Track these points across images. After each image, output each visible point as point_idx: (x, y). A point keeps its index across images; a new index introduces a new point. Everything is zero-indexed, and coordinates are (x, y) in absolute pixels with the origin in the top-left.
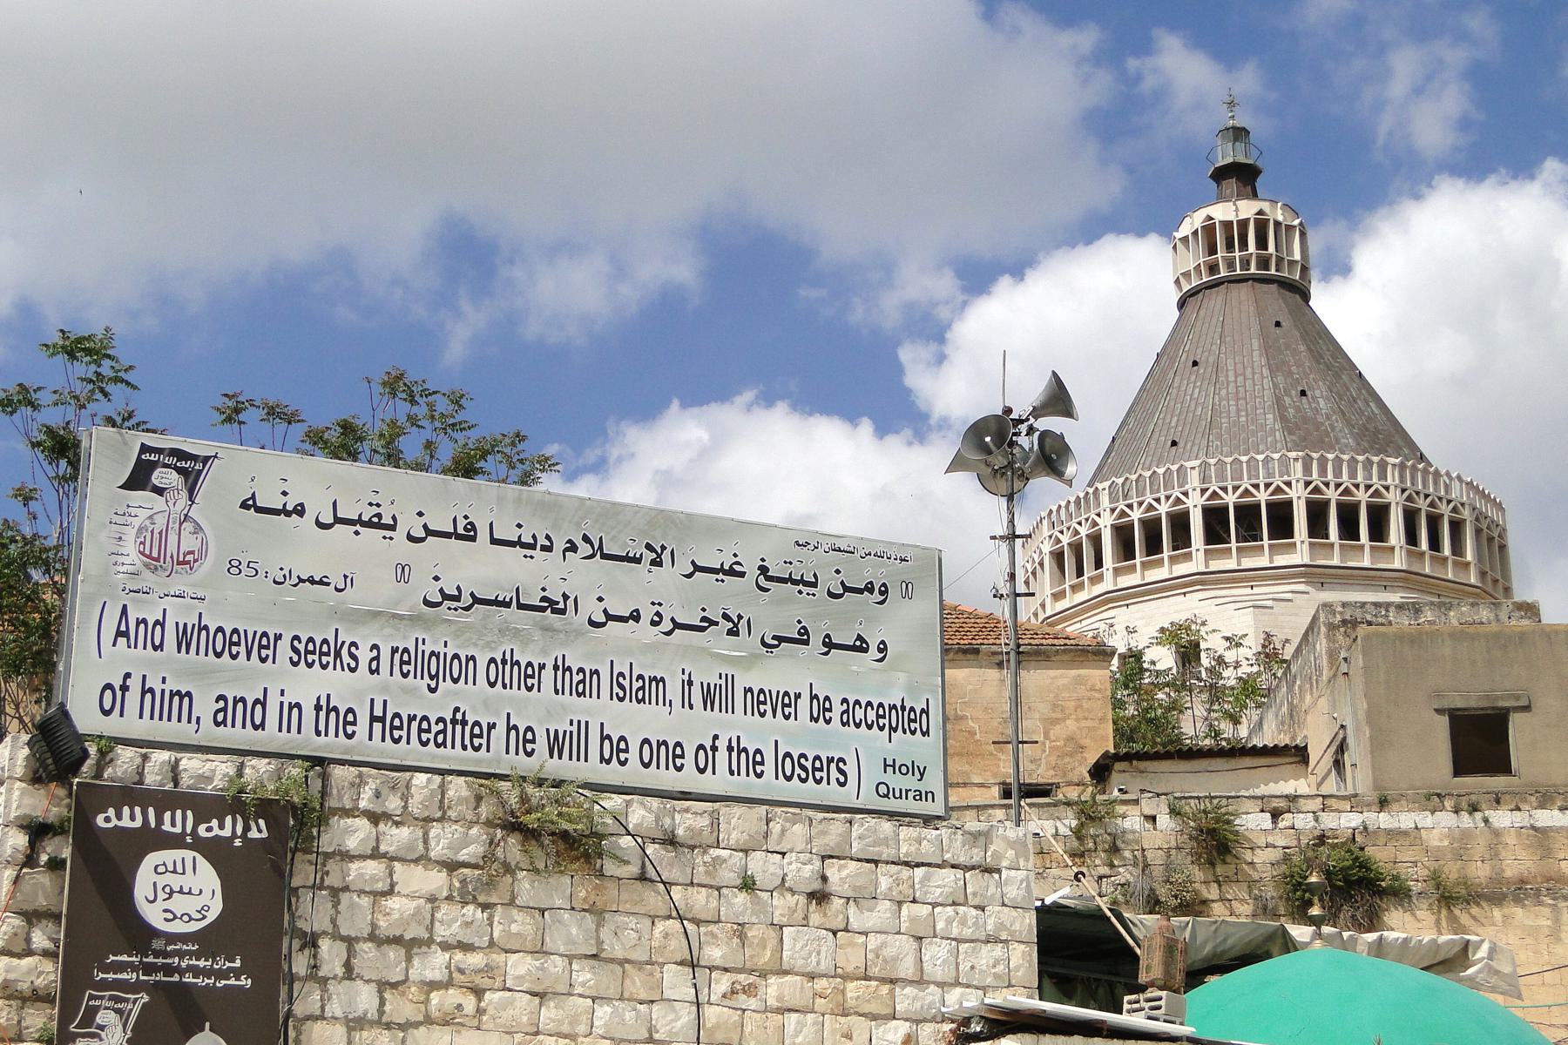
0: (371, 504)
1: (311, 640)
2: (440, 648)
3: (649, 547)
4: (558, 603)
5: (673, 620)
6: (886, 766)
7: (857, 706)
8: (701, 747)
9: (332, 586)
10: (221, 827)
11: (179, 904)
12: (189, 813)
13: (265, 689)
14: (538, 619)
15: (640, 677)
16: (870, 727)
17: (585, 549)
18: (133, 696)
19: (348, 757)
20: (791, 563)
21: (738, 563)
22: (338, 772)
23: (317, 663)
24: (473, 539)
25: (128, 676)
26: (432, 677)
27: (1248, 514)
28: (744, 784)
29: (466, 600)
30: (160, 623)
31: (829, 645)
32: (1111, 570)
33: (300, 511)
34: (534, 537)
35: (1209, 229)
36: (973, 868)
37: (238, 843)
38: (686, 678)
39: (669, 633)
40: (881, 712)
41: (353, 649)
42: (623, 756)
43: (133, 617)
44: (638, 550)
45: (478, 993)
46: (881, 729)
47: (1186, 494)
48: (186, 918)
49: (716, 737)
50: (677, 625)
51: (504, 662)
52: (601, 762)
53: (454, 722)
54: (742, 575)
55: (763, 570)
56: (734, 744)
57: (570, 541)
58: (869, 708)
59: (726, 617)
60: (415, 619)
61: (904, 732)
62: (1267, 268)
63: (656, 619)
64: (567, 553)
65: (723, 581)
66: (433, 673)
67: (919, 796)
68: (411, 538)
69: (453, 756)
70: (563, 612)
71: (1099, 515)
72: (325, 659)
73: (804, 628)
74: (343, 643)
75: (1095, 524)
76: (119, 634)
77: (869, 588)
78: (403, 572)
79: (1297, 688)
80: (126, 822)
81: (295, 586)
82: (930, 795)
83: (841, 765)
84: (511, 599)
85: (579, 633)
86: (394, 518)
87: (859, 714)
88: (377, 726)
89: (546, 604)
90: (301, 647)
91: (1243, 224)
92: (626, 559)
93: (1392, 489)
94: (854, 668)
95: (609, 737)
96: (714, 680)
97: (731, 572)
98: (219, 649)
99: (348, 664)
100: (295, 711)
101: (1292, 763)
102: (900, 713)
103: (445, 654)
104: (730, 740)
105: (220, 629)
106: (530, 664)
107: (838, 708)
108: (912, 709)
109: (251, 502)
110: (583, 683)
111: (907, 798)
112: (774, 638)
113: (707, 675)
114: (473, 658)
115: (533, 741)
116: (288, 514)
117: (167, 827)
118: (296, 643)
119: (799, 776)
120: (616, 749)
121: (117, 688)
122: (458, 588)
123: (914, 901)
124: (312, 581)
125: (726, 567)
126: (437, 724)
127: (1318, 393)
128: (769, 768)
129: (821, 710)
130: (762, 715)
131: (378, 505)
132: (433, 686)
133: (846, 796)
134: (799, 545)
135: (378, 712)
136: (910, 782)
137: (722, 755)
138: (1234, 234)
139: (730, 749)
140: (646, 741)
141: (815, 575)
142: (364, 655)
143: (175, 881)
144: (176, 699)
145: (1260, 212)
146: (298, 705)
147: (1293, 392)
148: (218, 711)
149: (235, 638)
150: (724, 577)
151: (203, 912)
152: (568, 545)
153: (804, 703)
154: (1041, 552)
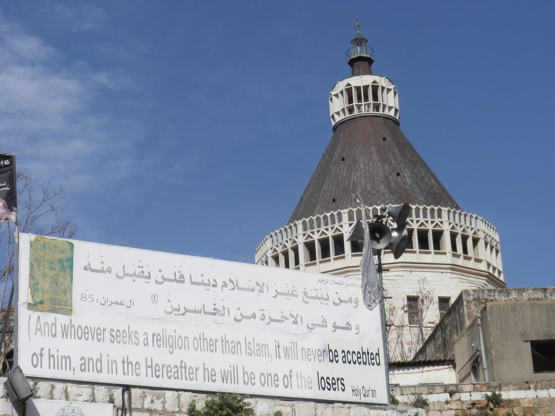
1: (118, 331)
2: (173, 333)
3: (257, 284)
4: (221, 311)
5: (270, 317)
7: (349, 354)
8: (285, 376)
9: (125, 305)
15: (258, 344)
16: (355, 363)
17: (231, 286)
18: (45, 358)
21: (294, 290)
24: (183, 282)
25: (42, 349)
26: (170, 347)
30: (54, 324)
31: (336, 327)
32: (304, 266)
33: (109, 271)
34: (209, 280)
35: (349, 91)
38: (277, 344)
39: (268, 324)
40: (359, 356)
41: (136, 334)
43: (42, 320)
44: (253, 285)
47: (341, 226)
51: (200, 339)
52: (244, 384)
53: (181, 367)
54: (297, 296)
55: (305, 293)
56: (299, 374)
57: (224, 282)
58: (354, 354)
59: (291, 315)
62: (378, 110)
63: (263, 317)
64: (223, 288)
65: (289, 299)
66: (171, 345)
71: (297, 237)
72: (125, 340)
74: (132, 332)
75: (295, 242)
76: (37, 330)
77: (350, 300)
78: (155, 298)
79: (448, 331)
81: (110, 305)
84: (201, 310)
86: (149, 273)
87: (350, 357)
88: (149, 370)
90: (114, 334)
91: (366, 88)
93: (444, 223)
96: (288, 345)
97: (293, 295)
98: (80, 336)
99: (135, 342)
101: (447, 368)
103: (175, 336)
104: (297, 373)
105: (80, 327)
106: (211, 340)
107: (341, 355)
112: (312, 324)
113: (285, 342)
115: (215, 375)
116: (104, 272)
122: (179, 305)
124: (117, 303)
125: (290, 292)
126: (174, 368)
127: (406, 174)
130: (310, 360)
131: (142, 267)
132: (171, 351)
134: (320, 281)
139: (297, 376)
142: (141, 337)
144: (64, 359)
145: (375, 82)
146: (115, 361)
147: (393, 174)
148: (81, 365)
149: (86, 331)
150: (289, 297)
152: (223, 284)
154: (266, 257)
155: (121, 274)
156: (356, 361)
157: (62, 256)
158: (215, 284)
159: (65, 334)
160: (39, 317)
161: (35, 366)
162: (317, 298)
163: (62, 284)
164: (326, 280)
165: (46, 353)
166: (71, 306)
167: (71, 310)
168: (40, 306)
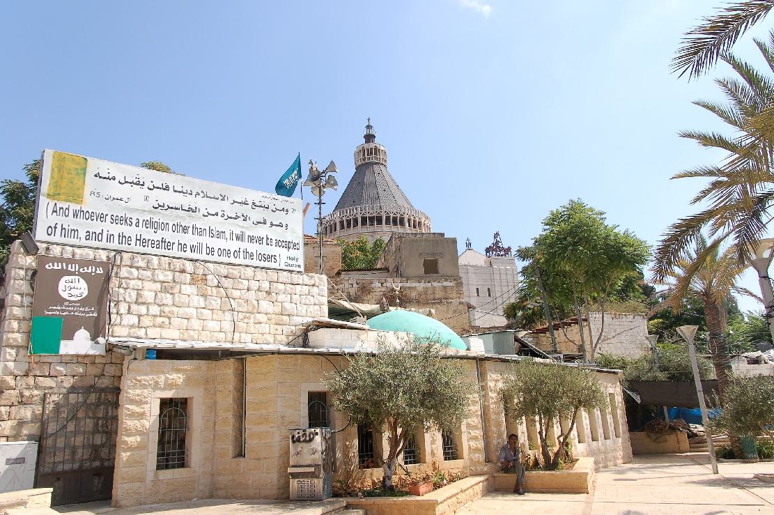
12: (77, 265)
17: (202, 195)
24: (168, 190)
27: (372, 219)
28: (248, 262)
31: (272, 225)
33: (114, 179)
43: (58, 206)
45: (169, 318)
55: (254, 203)
59: (243, 216)
69: (159, 252)
76: (54, 211)
80: (56, 267)
87: (280, 244)
88: (138, 242)
96: (239, 233)
105: (88, 212)
107: (274, 242)
110: (200, 232)
113: (237, 231)
116: (110, 179)
117: (70, 269)
120: (211, 251)
133: (276, 266)
135: (139, 238)
138: (370, 152)
142: (134, 221)
143: (72, 285)
157: (78, 167)
159: (75, 215)
162: (260, 206)
165: (59, 227)
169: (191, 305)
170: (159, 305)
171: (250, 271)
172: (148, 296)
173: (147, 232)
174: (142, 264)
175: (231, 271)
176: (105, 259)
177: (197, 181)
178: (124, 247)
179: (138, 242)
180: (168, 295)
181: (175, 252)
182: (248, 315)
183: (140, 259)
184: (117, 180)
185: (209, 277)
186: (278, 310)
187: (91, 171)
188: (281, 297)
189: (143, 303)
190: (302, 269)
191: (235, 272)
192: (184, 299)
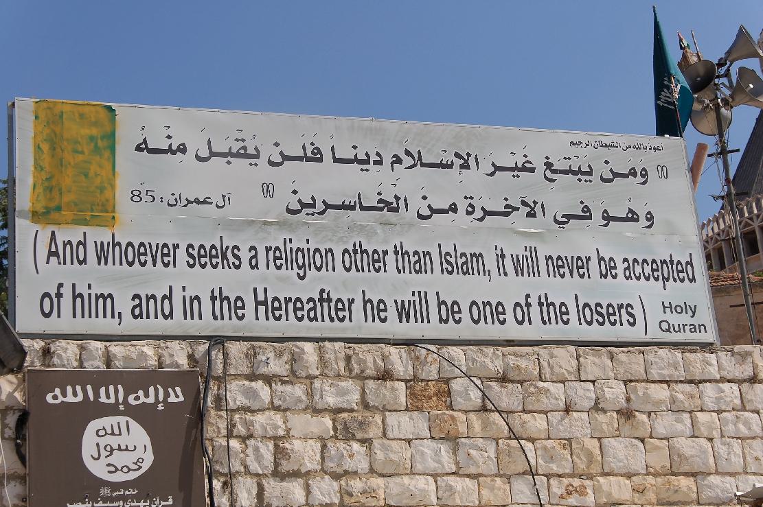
0: (237, 140)
1: (202, 246)
2: (304, 245)
3: (457, 155)
6: (664, 307)
8: (517, 304)
9: (214, 204)
10: (147, 395)
11: (119, 459)
12: (120, 387)
13: (171, 287)
14: (378, 216)
15: (463, 255)
16: (648, 279)
17: (408, 161)
18: (67, 301)
19: (241, 334)
20: (569, 159)
21: (528, 162)
22: (235, 349)
23: (209, 263)
24: (320, 160)
25: (61, 285)
26: (300, 268)
28: (555, 331)
29: (320, 206)
30: (83, 243)
33: (182, 149)
34: (367, 154)
36: (745, 381)
37: (160, 407)
38: (499, 252)
39: (481, 219)
40: (655, 267)
41: (236, 251)
42: (457, 317)
46: (657, 279)
48: (125, 470)
49: (528, 296)
50: (487, 213)
51: (355, 252)
53: (321, 300)
54: (532, 170)
56: (543, 300)
59: (524, 203)
60: (280, 224)
61: (675, 280)
63: (470, 209)
64: (395, 165)
65: (518, 176)
67: (694, 329)
68: (271, 163)
69: (323, 327)
70: (396, 210)
72: (214, 261)
73: (586, 207)
74: (227, 247)
76: (51, 254)
77: (633, 173)
78: (268, 190)
80: (70, 398)
81: (185, 206)
82: (702, 328)
83: (629, 309)
85: (411, 225)
86: (256, 149)
87: (638, 269)
88: (262, 309)
89: (382, 205)
90: (195, 253)
92: (441, 165)
94: (629, 234)
95: (444, 303)
96: (521, 252)
97: (524, 169)
98: (130, 259)
100: (195, 302)
102: (670, 266)
104: (540, 297)
105: (130, 244)
106: (375, 251)
107: (621, 267)
108: (679, 262)
109: (143, 146)
110: (420, 262)
111: (685, 331)
113: (514, 248)
114: (330, 250)
115: (385, 310)
116: (174, 153)
117: (103, 399)
118: (190, 250)
119: (597, 320)
120: (451, 311)
121: (53, 296)
122: (313, 198)
123: (702, 410)
124: (197, 201)
125: (520, 165)
126: (308, 303)
128: (573, 316)
129: (608, 270)
130: (563, 276)
131: (243, 140)
132: (302, 274)
133: (636, 334)
134: (574, 144)
135: (261, 298)
136: (685, 318)
137: (535, 309)
139: (540, 304)
140: (474, 303)
141: (589, 166)
142: (245, 255)
143: (113, 441)
144: (101, 300)
146: (197, 298)
148: (135, 307)
149: (142, 250)
150: (519, 174)
151: (138, 463)
152: (395, 159)
153: (594, 263)
155: (204, 153)
156: (649, 274)
157: (94, 131)
158: (379, 159)
159: (102, 256)
160: (53, 233)
161: (47, 315)
163: (97, 175)
164: (584, 142)
165: (67, 292)
166: (114, 211)
167: (114, 217)
168: (55, 215)
169: (419, 467)
170: (336, 476)
171: (564, 358)
172: (306, 453)
173: (281, 279)
174: (277, 366)
175: (512, 360)
176: (183, 362)
177: (392, 126)
178: (227, 326)
179: (262, 309)
180: (356, 446)
181: (359, 325)
182: (576, 482)
183: (271, 355)
184: (191, 152)
185: (457, 385)
186: (660, 460)
187: (127, 138)
188: (663, 424)
189: (296, 474)
190: (710, 336)
191: (524, 362)
192: (400, 452)
